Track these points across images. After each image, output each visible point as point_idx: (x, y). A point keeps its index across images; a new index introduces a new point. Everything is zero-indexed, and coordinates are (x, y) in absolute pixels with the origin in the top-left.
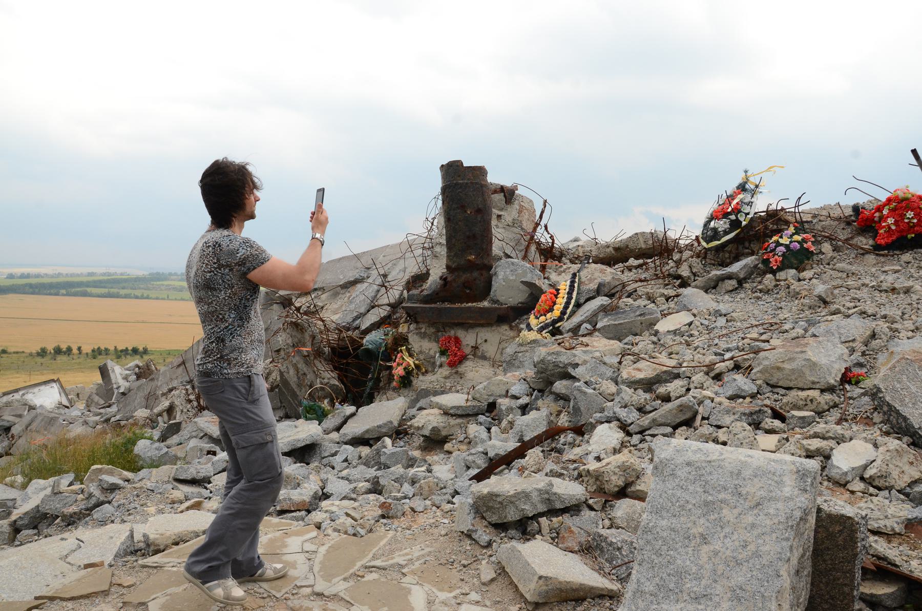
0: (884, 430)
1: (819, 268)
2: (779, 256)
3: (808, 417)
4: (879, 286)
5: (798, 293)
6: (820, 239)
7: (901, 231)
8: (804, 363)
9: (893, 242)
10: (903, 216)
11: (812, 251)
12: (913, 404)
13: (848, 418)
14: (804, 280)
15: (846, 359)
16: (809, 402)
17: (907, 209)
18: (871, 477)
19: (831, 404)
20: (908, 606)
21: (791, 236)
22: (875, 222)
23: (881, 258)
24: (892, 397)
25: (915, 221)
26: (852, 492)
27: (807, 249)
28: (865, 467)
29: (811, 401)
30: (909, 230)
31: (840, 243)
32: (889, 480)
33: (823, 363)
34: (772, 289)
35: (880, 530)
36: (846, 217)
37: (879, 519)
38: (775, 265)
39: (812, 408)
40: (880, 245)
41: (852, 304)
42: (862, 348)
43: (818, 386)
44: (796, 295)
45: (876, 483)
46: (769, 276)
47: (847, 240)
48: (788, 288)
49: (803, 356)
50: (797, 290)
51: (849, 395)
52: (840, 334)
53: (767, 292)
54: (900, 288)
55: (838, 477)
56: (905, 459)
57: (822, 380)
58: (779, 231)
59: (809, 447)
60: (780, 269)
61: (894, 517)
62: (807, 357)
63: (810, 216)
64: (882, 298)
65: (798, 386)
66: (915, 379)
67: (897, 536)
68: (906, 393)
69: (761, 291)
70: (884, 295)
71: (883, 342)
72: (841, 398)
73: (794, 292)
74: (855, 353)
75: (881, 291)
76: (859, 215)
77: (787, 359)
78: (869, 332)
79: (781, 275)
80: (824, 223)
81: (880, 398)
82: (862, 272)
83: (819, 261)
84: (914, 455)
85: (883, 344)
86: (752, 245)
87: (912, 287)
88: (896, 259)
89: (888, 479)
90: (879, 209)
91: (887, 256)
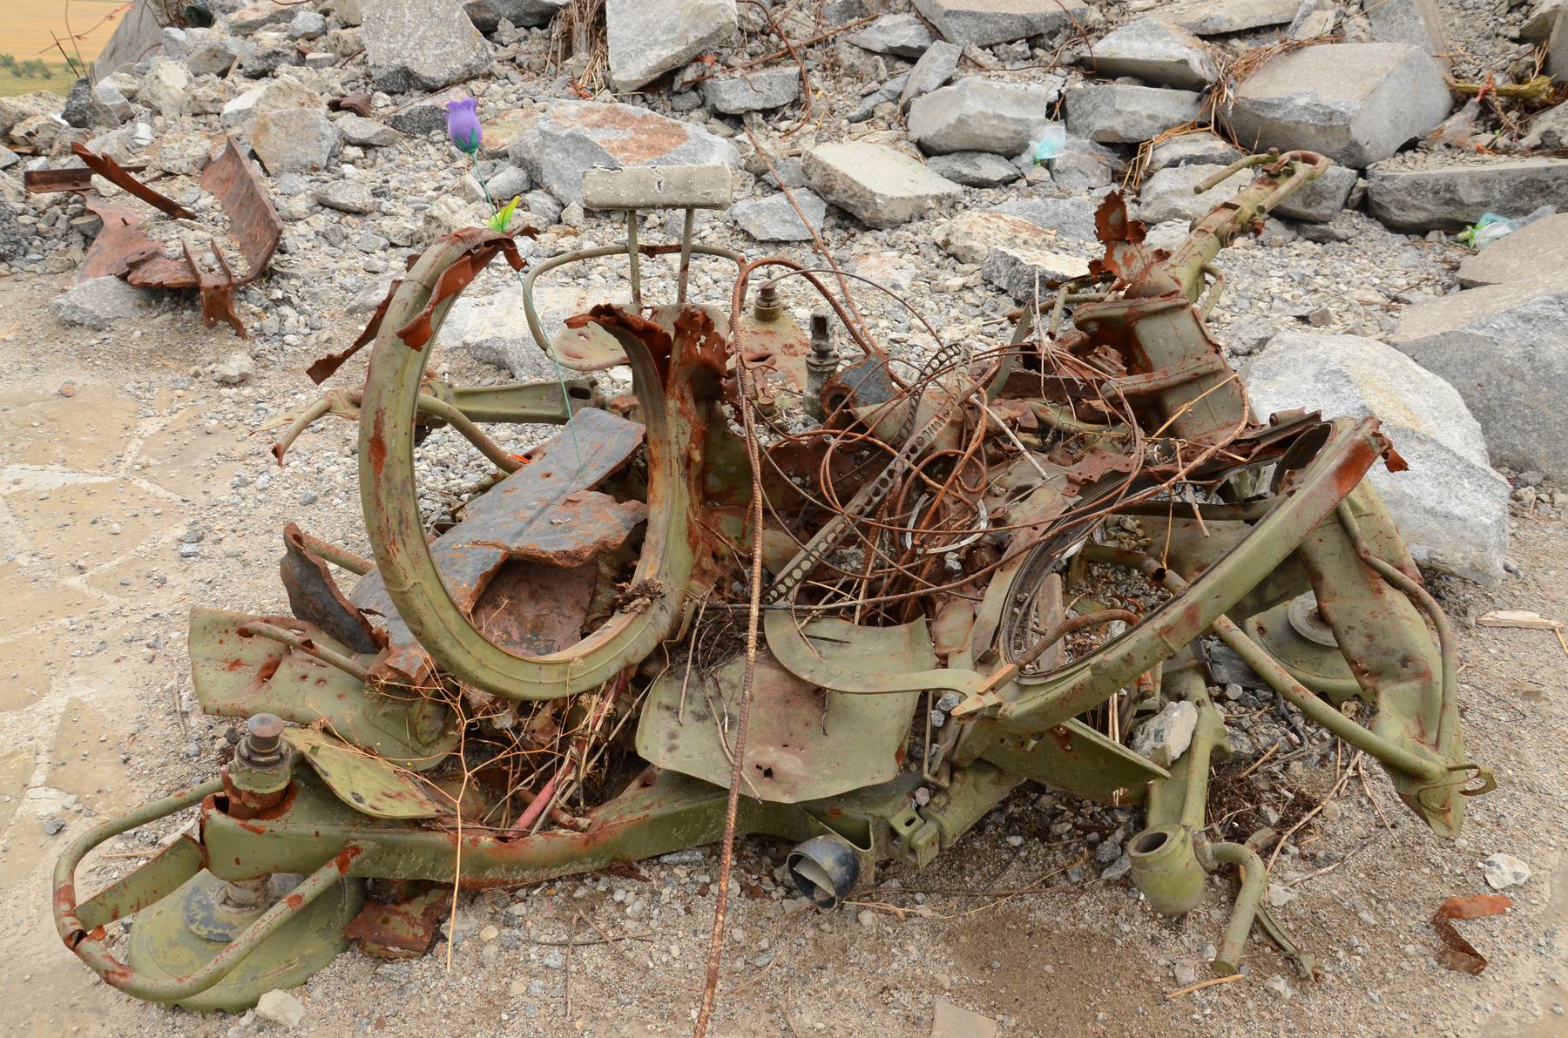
56: (294, 99)
61: (189, 156)
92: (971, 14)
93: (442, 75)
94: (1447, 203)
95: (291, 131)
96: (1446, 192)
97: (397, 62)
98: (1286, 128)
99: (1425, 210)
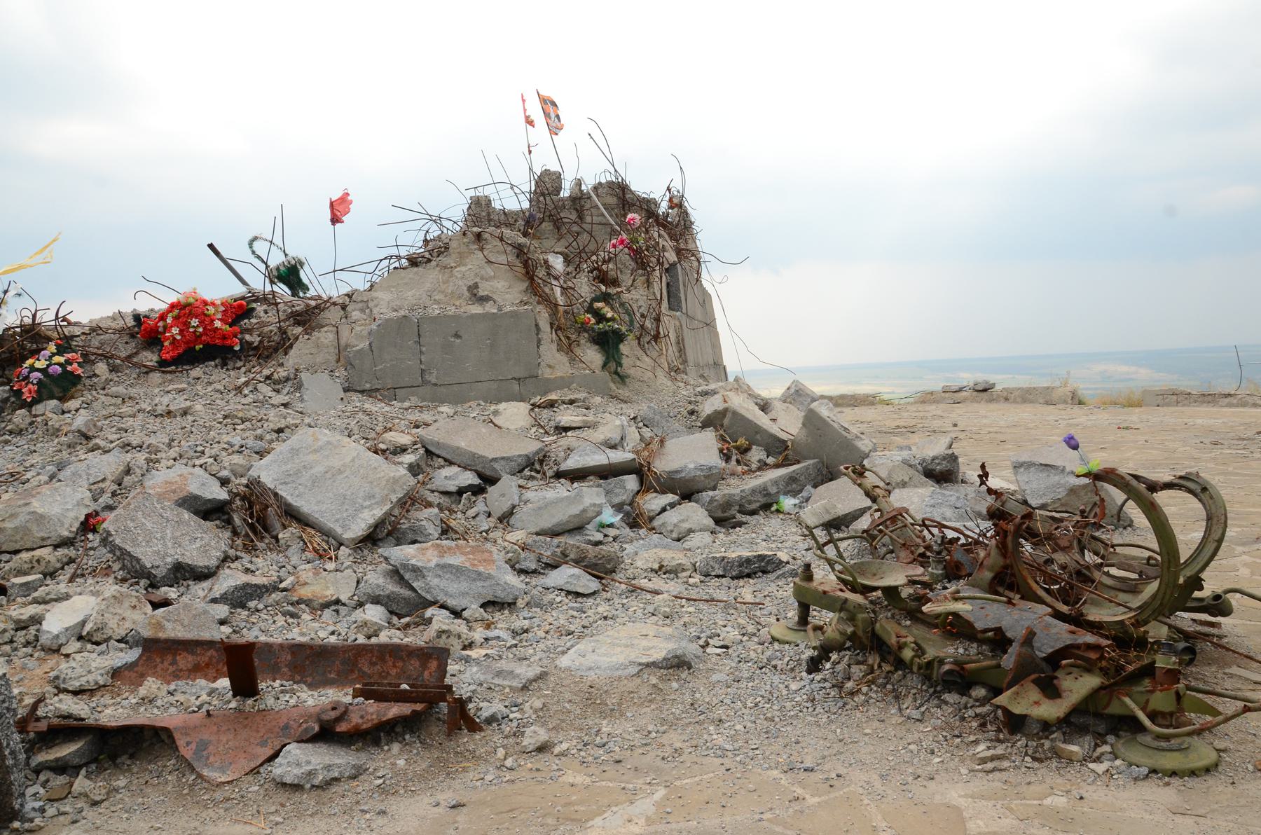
0: (119, 577)
1: (91, 395)
2: (34, 385)
3: (33, 581)
4: (155, 411)
5: (58, 430)
6: (93, 358)
7: (188, 342)
8: (28, 517)
9: (180, 356)
10: (187, 325)
11: (79, 375)
12: (148, 542)
13: (85, 572)
14: (69, 412)
15: (88, 503)
16: (35, 564)
17: (191, 315)
18: (88, 633)
19: (65, 560)
20: (101, 757)
21: (50, 357)
22: (160, 333)
23: (168, 375)
24: (123, 540)
25: (201, 330)
26: (67, 656)
27: (72, 373)
28: (83, 623)
29: (38, 561)
30: (196, 340)
31: (119, 361)
32: (106, 631)
33: (53, 513)
34: (27, 429)
35: (82, 688)
36: (129, 328)
37: (82, 676)
38: (28, 397)
39: (40, 570)
40: (165, 360)
41: (118, 436)
42: (111, 487)
43: (49, 542)
44: (56, 432)
45: (95, 639)
46: (23, 411)
47: (129, 358)
48: (46, 424)
49: (27, 509)
50: (57, 426)
51: (90, 545)
52: (88, 474)
53: (20, 432)
54: (176, 411)
55: (49, 643)
56: (126, 604)
57: (53, 533)
58: (35, 353)
59: (22, 617)
60: (36, 401)
61: (97, 669)
62: (32, 510)
63: (88, 328)
64: (154, 424)
65: (26, 546)
66: (152, 514)
67: (102, 689)
68: (139, 532)
69: (11, 432)
70: (158, 420)
71: (136, 476)
72: (78, 550)
73: (53, 428)
74: (104, 495)
75: (156, 416)
76: (142, 324)
77: (7, 515)
78: (122, 468)
79: (38, 409)
80: (102, 337)
81: (111, 542)
82: (142, 394)
83: (92, 386)
84: (136, 597)
85: (136, 480)
86: (7, 372)
87: (190, 407)
88: (185, 375)
89: (105, 631)
90: (163, 317)
91: (175, 372)
92: (503, 458)
93: (214, 562)
94: (765, 496)
95: (186, 622)
96: (764, 490)
97: (169, 560)
98: (688, 481)
99: (759, 501)
